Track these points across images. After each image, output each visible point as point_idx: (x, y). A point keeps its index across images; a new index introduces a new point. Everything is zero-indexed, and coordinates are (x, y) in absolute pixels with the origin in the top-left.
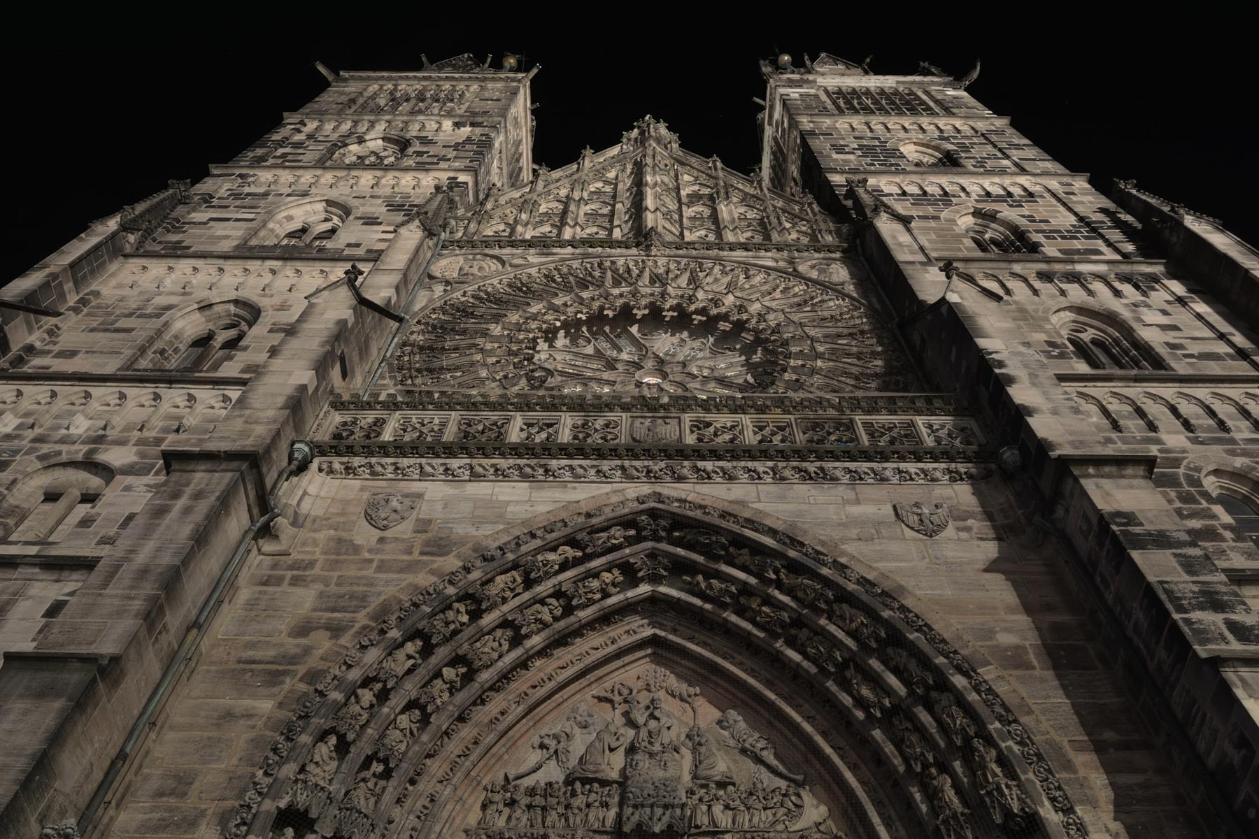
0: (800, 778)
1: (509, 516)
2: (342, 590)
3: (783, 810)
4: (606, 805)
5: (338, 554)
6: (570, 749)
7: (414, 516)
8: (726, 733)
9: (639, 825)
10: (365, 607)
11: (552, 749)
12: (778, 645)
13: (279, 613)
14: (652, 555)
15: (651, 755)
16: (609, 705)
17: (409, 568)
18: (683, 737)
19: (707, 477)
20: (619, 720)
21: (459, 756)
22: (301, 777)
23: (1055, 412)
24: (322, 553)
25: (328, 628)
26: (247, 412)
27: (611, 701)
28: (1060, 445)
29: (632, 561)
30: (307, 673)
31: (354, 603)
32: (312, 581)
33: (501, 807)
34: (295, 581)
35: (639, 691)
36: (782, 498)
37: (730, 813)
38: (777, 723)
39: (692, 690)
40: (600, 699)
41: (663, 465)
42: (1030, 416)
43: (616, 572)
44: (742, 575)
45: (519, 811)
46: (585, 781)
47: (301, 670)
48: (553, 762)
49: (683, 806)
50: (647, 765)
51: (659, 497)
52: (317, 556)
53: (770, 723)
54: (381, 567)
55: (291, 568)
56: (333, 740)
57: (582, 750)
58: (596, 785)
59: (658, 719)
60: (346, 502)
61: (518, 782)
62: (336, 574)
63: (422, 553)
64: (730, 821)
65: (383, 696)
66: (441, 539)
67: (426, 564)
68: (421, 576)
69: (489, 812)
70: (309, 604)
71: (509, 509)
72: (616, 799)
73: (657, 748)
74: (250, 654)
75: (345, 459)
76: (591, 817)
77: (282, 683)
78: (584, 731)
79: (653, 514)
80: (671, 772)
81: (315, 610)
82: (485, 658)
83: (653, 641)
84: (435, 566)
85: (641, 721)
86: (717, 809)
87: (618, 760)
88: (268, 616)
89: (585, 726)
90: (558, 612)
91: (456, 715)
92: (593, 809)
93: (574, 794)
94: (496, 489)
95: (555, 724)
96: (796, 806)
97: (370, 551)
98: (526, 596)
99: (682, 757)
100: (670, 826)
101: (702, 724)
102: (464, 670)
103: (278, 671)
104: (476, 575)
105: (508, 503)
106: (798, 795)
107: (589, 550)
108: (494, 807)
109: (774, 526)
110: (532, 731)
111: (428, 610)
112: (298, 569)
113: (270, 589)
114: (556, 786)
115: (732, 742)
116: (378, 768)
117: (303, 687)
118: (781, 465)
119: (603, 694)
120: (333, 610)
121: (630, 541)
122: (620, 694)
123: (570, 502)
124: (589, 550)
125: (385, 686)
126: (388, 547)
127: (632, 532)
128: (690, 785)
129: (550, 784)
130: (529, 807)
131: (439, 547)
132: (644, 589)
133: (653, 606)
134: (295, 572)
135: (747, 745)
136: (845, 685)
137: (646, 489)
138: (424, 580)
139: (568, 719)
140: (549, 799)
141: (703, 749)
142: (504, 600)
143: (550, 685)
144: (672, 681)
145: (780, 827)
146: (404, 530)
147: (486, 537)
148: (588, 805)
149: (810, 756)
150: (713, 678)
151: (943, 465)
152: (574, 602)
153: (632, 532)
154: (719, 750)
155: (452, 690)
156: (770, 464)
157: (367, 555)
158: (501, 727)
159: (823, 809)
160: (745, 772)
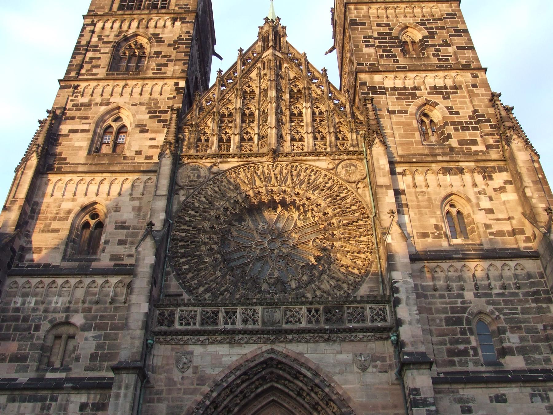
1: (223, 363)
2: (175, 404)
5: (170, 386)
14: (272, 373)
19: (291, 341)
23: (410, 324)
24: (165, 386)
26: (130, 331)
28: (408, 344)
34: (159, 400)
36: (315, 351)
41: (274, 337)
42: (401, 326)
51: (272, 351)
52: (164, 387)
54: (185, 393)
55: (156, 394)
60: (168, 358)
62: (171, 396)
63: (197, 385)
66: (202, 377)
68: (198, 396)
75: (164, 337)
79: (272, 359)
94: (218, 348)
97: (180, 384)
98: (231, 396)
104: (215, 394)
105: (222, 355)
109: (311, 367)
111: (202, 412)
113: (151, 404)
118: (316, 335)
121: (264, 369)
123: (243, 355)
124: (251, 377)
126: (186, 382)
127: (265, 366)
131: (202, 381)
134: (158, 396)
137: (269, 347)
138: (199, 398)
142: (225, 400)
146: (189, 373)
147: (217, 374)
151: (373, 334)
153: (265, 366)
156: (312, 335)
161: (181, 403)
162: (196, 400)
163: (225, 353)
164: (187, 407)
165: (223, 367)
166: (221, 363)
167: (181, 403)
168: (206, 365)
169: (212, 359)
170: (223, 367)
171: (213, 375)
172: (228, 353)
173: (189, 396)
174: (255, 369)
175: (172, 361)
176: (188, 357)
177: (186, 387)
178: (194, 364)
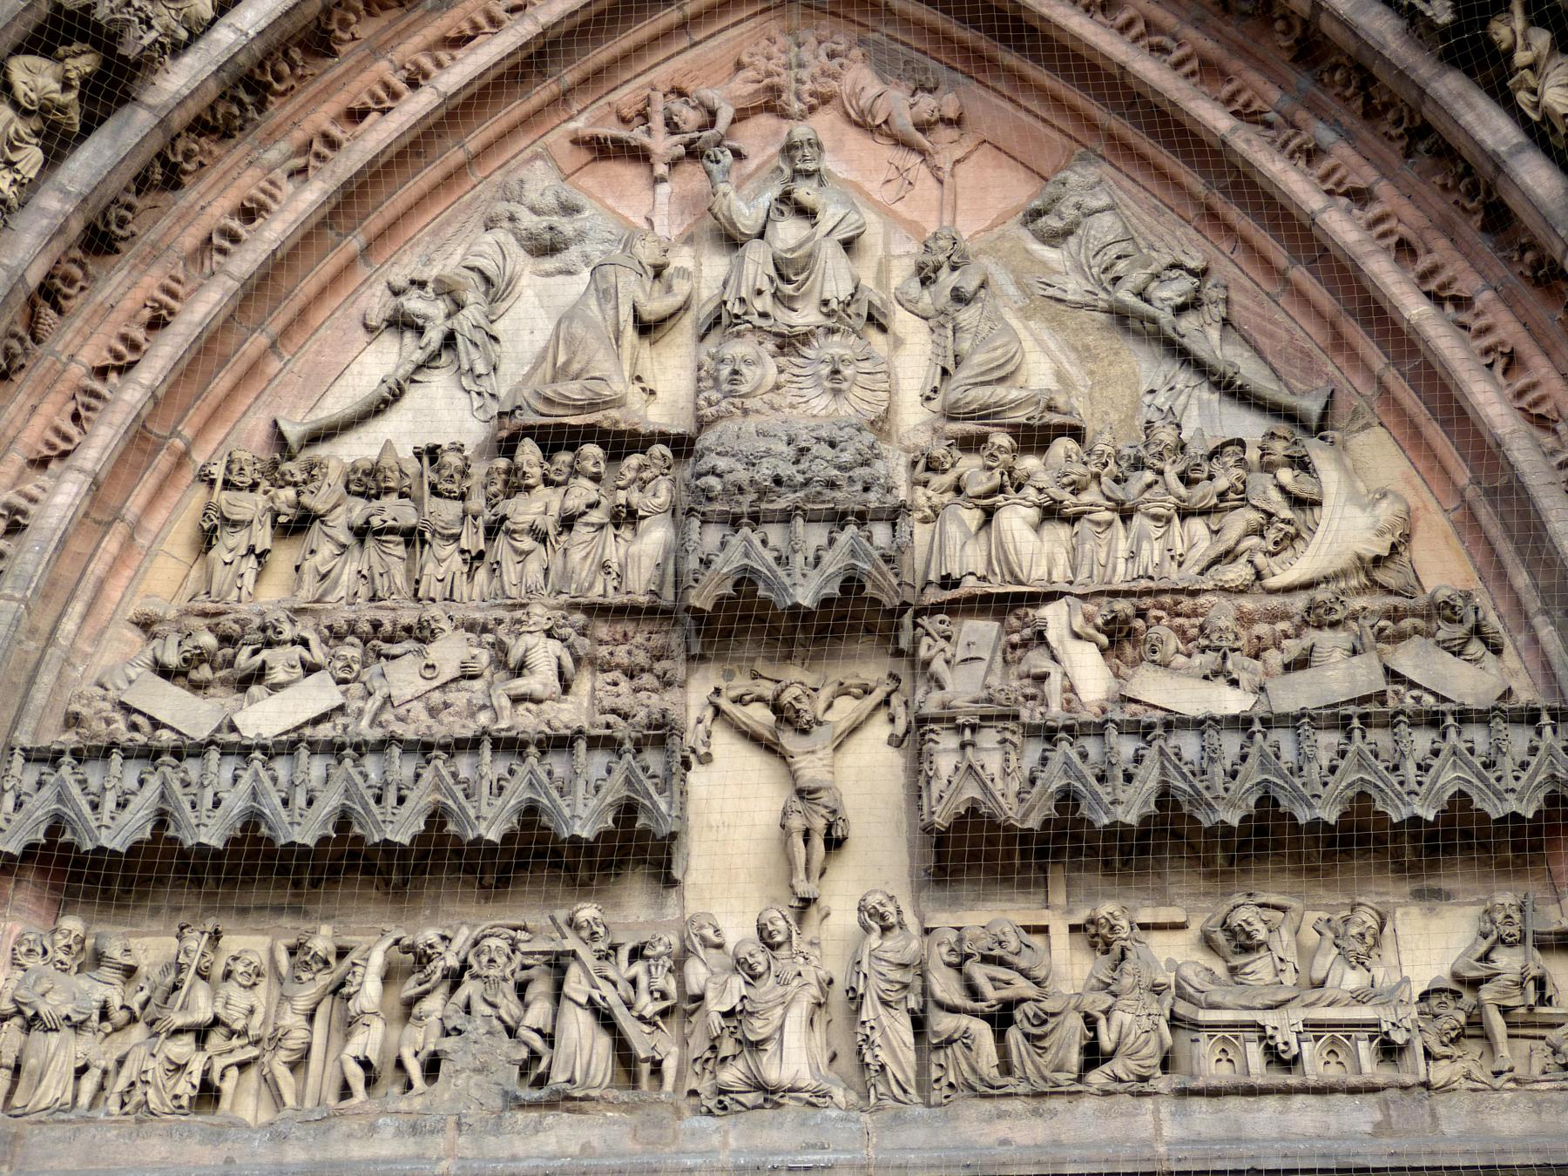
4: (626, 517)
6: (498, 328)
9: (746, 580)
15: (788, 343)
18: (901, 274)
21: (102, 372)
27: (639, 155)
33: (263, 537)
35: (741, 116)
38: (1234, 214)
40: (602, 150)
45: (327, 550)
46: (555, 440)
48: (439, 382)
49: (894, 515)
50: (772, 375)
53: (1212, 215)
57: (544, 330)
58: (592, 450)
59: (806, 213)
61: (321, 451)
64: (1062, 559)
69: (219, 553)
73: (806, 317)
78: (549, 264)
80: (857, 404)
85: (747, 215)
86: (1016, 519)
89: (545, 247)
91: (76, 227)
92: (581, 532)
93: (515, 484)
95: (449, 245)
96: (1297, 502)
99: (898, 343)
100: (852, 584)
101: (967, 228)
106: (1302, 464)
108: (240, 540)
110: (363, 271)
114: (452, 459)
119: (611, 130)
128: (923, 439)
129: (432, 454)
130: (361, 533)
136: (1493, 73)
139: (490, 225)
140: (432, 504)
143: (417, 105)
144: (860, 80)
145: (1237, 573)
148: (568, 522)
149: (1353, 331)
150: (1010, 59)
154: (1025, 314)
155: (58, 143)
158: (246, 261)
160: (1121, 391)
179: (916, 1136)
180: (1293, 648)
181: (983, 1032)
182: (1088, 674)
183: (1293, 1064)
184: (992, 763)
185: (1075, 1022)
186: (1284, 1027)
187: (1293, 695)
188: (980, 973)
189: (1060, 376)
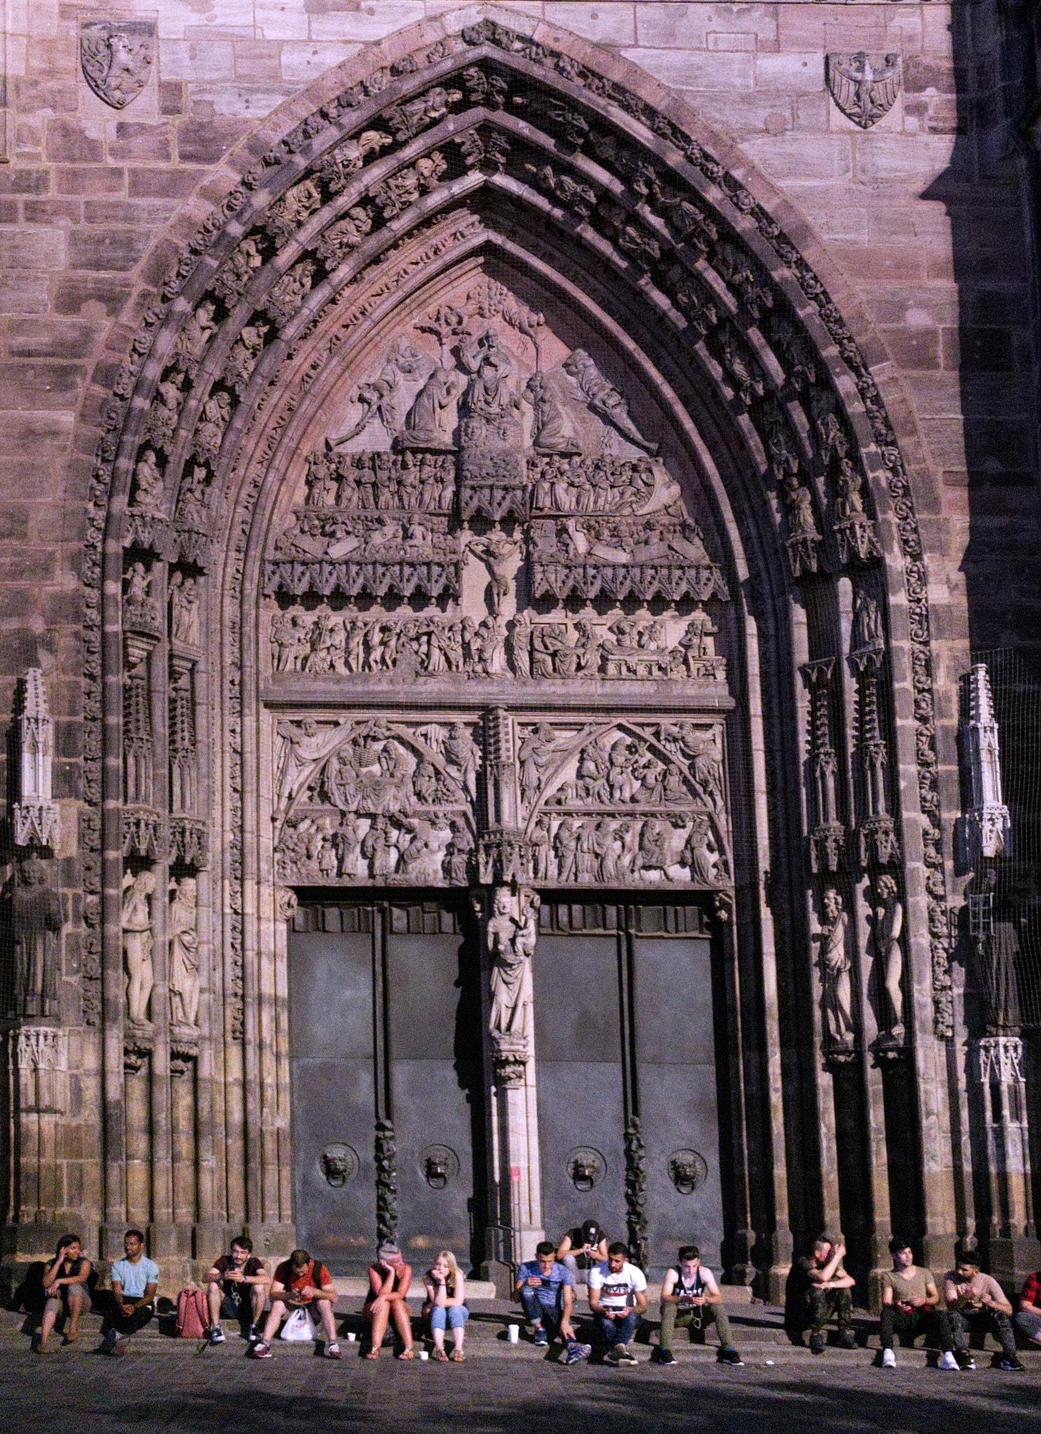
0: (654, 446)
2: (99, 228)
3: (630, 490)
7: (153, 80)
8: (573, 380)
10: (135, 260)
11: (374, 401)
12: (642, 282)
13: (32, 272)
16: (435, 338)
17: (173, 185)
20: (450, 362)
22: (136, 511)
24: (54, 157)
25: (100, 298)
29: (458, 140)
30: (97, 369)
31: (120, 254)
32: (55, 213)
34: (35, 213)
37: (574, 491)
39: (534, 318)
43: (437, 156)
44: (602, 175)
47: (89, 363)
52: (45, 164)
56: (151, 457)
60: (48, 45)
62: (81, 198)
63: (185, 157)
65: (187, 386)
66: (202, 126)
67: (194, 177)
68: (192, 200)
70: (63, 256)
71: (285, 59)
72: (452, 475)
73: (494, 409)
74: (20, 341)
76: (427, 497)
77: (73, 386)
81: (74, 266)
82: (287, 309)
83: (487, 249)
84: (206, 182)
85: (474, 365)
86: (561, 487)
87: (450, 419)
88: (20, 278)
90: (366, 227)
97: (113, 152)
98: (326, 213)
99: (523, 414)
101: (545, 368)
102: (265, 329)
103: (63, 368)
105: (281, 43)
107: (401, 137)
112: (28, 189)
115: (580, 394)
116: (200, 473)
117: (98, 390)
120: (98, 266)
122: (448, 324)
123: (366, 43)
124: (401, 137)
125: (187, 377)
131: (203, 142)
132: (474, 179)
133: (485, 202)
135: (597, 402)
138: (199, 209)
141: (546, 408)
142: (300, 224)
144: (511, 303)
147: (262, 120)
149: (668, 423)
152: (387, 214)
157: (111, 162)
159: (676, 489)
161: (128, 226)
162: (187, 221)
163: (287, 35)
164: (153, 242)
165: (287, 93)
166: (275, 75)
167: (128, 226)
168: (212, 82)
169: (236, 57)
170: (287, 93)
171: (246, 121)
172: (304, 36)
173: (157, 202)
174: (418, 106)
175: (71, 62)
176: (136, 41)
177: (138, 165)
178: (165, 77)
179: (530, 690)
180: (643, 536)
181: (549, 659)
182: (580, 542)
183: (635, 672)
184: (552, 578)
185: (575, 659)
186: (632, 661)
187: (643, 555)
188: (548, 641)
189: (575, 430)
